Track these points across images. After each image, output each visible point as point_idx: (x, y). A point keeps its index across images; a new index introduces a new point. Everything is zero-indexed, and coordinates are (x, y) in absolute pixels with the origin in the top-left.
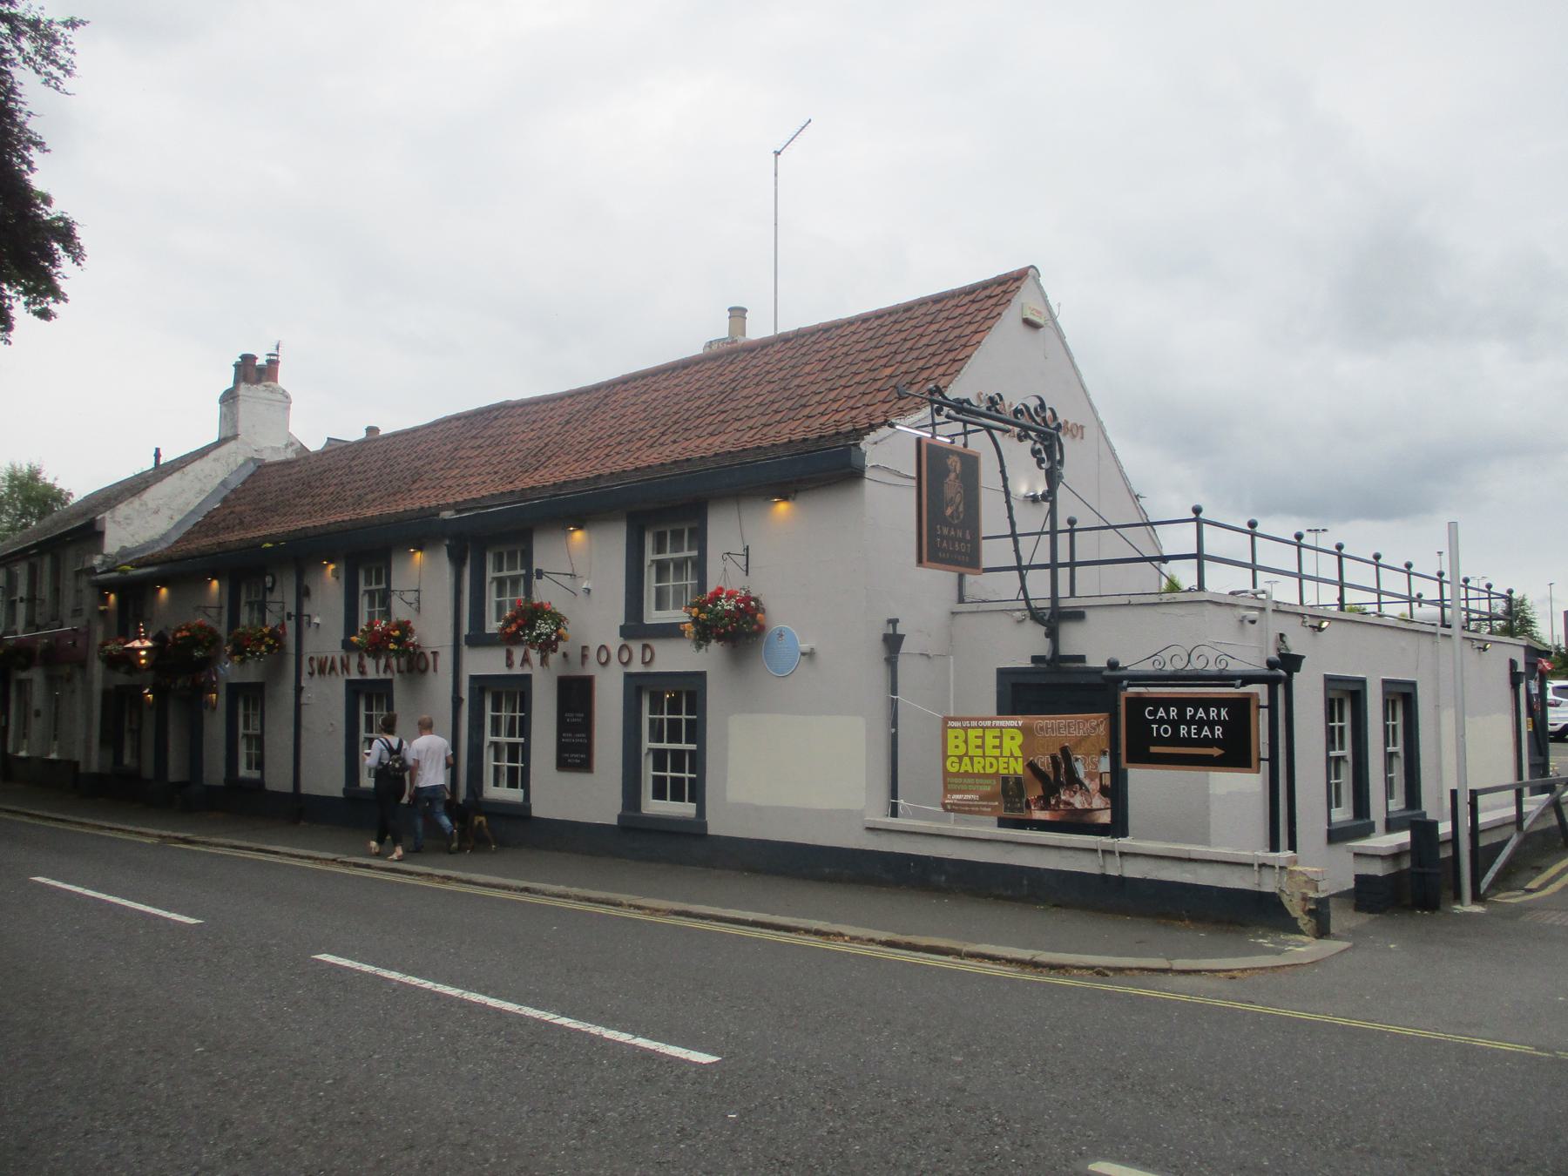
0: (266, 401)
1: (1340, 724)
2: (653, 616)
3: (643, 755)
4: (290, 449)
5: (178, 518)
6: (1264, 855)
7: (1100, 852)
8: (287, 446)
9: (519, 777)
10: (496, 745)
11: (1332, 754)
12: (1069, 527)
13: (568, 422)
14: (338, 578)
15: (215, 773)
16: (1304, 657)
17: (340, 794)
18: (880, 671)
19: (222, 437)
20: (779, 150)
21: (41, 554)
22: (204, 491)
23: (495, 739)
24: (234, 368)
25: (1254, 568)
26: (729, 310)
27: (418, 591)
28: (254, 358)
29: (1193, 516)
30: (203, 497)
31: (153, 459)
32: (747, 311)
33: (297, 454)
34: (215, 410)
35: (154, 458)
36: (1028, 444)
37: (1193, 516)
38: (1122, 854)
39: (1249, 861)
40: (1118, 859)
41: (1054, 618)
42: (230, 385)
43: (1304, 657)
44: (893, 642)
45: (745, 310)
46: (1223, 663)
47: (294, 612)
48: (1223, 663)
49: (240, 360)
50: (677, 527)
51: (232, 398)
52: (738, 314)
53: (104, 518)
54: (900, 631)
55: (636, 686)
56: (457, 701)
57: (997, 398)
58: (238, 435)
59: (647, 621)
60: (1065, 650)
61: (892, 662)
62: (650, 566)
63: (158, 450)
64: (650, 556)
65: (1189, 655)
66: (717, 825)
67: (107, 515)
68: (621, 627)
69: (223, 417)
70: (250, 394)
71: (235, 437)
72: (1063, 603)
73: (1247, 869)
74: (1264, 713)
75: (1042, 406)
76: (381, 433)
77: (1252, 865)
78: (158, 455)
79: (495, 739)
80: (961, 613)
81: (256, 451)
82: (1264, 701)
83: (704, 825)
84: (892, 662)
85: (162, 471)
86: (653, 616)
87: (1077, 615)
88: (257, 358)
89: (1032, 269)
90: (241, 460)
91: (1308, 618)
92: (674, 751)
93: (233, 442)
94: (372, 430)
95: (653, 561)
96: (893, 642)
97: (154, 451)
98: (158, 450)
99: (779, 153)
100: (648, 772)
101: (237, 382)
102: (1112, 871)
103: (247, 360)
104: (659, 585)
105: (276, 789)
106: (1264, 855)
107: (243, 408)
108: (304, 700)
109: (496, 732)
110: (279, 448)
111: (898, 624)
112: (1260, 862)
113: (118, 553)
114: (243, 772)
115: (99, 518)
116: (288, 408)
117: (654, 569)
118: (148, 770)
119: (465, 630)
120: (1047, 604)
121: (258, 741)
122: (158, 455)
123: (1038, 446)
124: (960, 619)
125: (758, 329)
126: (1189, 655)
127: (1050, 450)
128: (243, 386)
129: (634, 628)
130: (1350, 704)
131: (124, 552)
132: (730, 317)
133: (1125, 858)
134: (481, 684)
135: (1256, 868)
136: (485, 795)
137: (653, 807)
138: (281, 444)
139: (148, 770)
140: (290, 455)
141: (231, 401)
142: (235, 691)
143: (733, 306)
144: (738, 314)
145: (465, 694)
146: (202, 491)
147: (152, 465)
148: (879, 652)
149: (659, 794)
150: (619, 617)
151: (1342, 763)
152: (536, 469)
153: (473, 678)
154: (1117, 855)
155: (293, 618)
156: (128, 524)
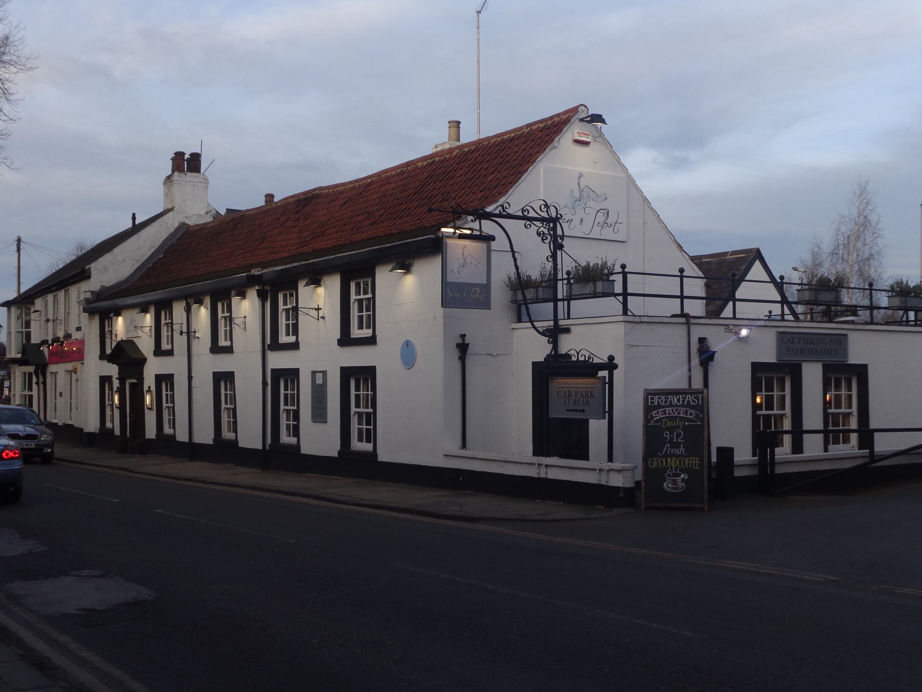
0: (192, 183)
1: (287, 392)
2: (356, 333)
3: (281, 412)
4: (209, 215)
5: (137, 265)
6: (607, 465)
7: (537, 465)
8: (207, 213)
9: (295, 431)
10: (288, 411)
11: (759, 412)
12: (566, 277)
13: (345, 203)
14: (207, 309)
15: (151, 432)
16: (716, 352)
17: (211, 442)
18: (457, 364)
19: (165, 209)
20: (480, 10)
21: (59, 289)
22: (153, 247)
23: (286, 407)
24: (171, 161)
25: (682, 297)
26: (449, 122)
27: (245, 317)
28: (183, 154)
29: (621, 270)
30: (155, 249)
31: (131, 221)
32: (460, 123)
33: (213, 218)
34: (160, 188)
35: (131, 220)
36: (534, 229)
37: (621, 270)
38: (547, 466)
39: (594, 468)
40: (544, 468)
41: (554, 333)
42: (170, 173)
43: (716, 352)
44: (463, 348)
45: (460, 123)
46: (591, 358)
47: (185, 330)
48: (591, 358)
49: (174, 155)
50: (365, 280)
51: (170, 182)
52: (456, 125)
53: (90, 268)
54: (466, 342)
55: (347, 373)
56: (265, 384)
57: (506, 205)
58: (174, 207)
59: (352, 336)
60: (563, 350)
61: (463, 359)
62: (354, 302)
63: (134, 215)
64: (353, 297)
65: (578, 354)
66: (384, 456)
67: (93, 266)
68: (338, 339)
69: (166, 195)
70: (181, 179)
71: (172, 209)
72: (561, 323)
73: (594, 472)
74: (607, 385)
75: (546, 206)
76: (276, 200)
77: (596, 470)
78: (134, 218)
79: (286, 407)
80: (516, 329)
81: (186, 217)
82: (607, 381)
83: (376, 455)
84: (463, 359)
85: (136, 228)
86: (356, 333)
87: (567, 330)
88: (185, 154)
89: (584, 107)
90: (176, 225)
91: (732, 327)
92: (366, 413)
93: (171, 213)
94: (269, 197)
95: (356, 300)
96: (463, 348)
97: (131, 216)
98: (134, 215)
99: (480, 12)
100: (355, 426)
101: (173, 171)
102: (543, 476)
103: (179, 156)
104: (360, 314)
105: (179, 440)
106: (607, 465)
107: (176, 188)
108: (193, 385)
109: (358, 406)
110: (202, 215)
111: (466, 337)
112: (600, 468)
113: (100, 290)
114: (167, 430)
115: (87, 267)
116: (206, 187)
117: (284, 314)
118: (117, 432)
119: (268, 341)
120: (551, 323)
121: (172, 411)
122: (134, 218)
123: (542, 229)
124: (516, 333)
125: (468, 136)
126: (578, 354)
127: (554, 229)
128: (176, 173)
129: (346, 340)
130: (790, 378)
131: (104, 290)
132: (449, 128)
133: (549, 468)
134: (278, 374)
135: (598, 471)
136: (281, 441)
137: (358, 445)
138: (203, 212)
139: (117, 432)
140: (209, 219)
141: (170, 184)
142: (160, 379)
143: (450, 120)
144: (456, 125)
145: (269, 382)
146: (152, 247)
147: (129, 225)
148: (456, 354)
149: (360, 439)
150: (337, 334)
151: (784, 418)
152: (317, 238)
153: (272, 370)
154: (544, 466)
155: (184, 334)
156: (106, 271)
